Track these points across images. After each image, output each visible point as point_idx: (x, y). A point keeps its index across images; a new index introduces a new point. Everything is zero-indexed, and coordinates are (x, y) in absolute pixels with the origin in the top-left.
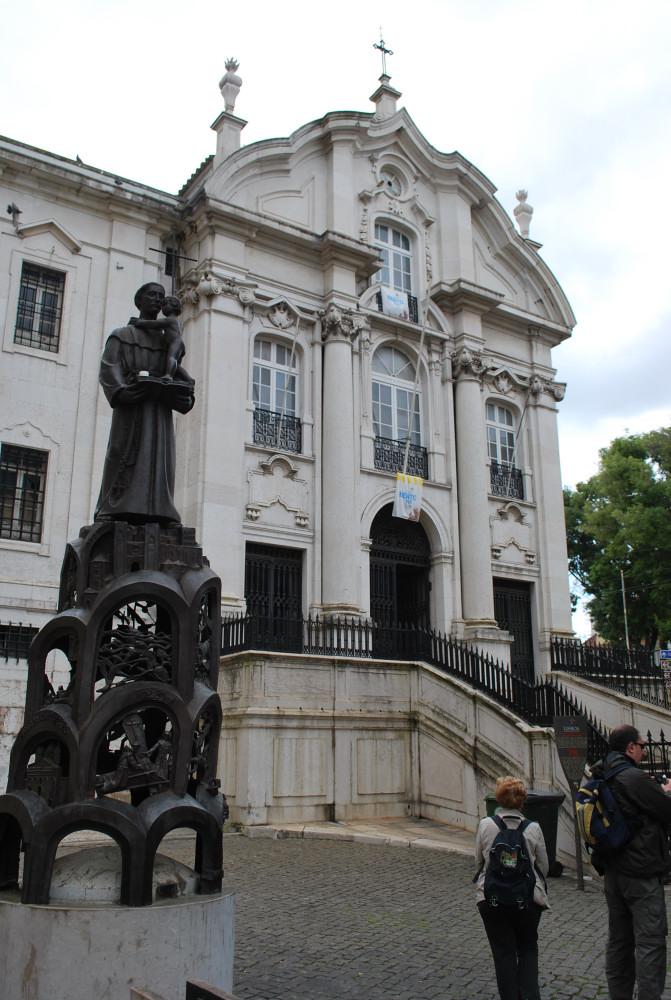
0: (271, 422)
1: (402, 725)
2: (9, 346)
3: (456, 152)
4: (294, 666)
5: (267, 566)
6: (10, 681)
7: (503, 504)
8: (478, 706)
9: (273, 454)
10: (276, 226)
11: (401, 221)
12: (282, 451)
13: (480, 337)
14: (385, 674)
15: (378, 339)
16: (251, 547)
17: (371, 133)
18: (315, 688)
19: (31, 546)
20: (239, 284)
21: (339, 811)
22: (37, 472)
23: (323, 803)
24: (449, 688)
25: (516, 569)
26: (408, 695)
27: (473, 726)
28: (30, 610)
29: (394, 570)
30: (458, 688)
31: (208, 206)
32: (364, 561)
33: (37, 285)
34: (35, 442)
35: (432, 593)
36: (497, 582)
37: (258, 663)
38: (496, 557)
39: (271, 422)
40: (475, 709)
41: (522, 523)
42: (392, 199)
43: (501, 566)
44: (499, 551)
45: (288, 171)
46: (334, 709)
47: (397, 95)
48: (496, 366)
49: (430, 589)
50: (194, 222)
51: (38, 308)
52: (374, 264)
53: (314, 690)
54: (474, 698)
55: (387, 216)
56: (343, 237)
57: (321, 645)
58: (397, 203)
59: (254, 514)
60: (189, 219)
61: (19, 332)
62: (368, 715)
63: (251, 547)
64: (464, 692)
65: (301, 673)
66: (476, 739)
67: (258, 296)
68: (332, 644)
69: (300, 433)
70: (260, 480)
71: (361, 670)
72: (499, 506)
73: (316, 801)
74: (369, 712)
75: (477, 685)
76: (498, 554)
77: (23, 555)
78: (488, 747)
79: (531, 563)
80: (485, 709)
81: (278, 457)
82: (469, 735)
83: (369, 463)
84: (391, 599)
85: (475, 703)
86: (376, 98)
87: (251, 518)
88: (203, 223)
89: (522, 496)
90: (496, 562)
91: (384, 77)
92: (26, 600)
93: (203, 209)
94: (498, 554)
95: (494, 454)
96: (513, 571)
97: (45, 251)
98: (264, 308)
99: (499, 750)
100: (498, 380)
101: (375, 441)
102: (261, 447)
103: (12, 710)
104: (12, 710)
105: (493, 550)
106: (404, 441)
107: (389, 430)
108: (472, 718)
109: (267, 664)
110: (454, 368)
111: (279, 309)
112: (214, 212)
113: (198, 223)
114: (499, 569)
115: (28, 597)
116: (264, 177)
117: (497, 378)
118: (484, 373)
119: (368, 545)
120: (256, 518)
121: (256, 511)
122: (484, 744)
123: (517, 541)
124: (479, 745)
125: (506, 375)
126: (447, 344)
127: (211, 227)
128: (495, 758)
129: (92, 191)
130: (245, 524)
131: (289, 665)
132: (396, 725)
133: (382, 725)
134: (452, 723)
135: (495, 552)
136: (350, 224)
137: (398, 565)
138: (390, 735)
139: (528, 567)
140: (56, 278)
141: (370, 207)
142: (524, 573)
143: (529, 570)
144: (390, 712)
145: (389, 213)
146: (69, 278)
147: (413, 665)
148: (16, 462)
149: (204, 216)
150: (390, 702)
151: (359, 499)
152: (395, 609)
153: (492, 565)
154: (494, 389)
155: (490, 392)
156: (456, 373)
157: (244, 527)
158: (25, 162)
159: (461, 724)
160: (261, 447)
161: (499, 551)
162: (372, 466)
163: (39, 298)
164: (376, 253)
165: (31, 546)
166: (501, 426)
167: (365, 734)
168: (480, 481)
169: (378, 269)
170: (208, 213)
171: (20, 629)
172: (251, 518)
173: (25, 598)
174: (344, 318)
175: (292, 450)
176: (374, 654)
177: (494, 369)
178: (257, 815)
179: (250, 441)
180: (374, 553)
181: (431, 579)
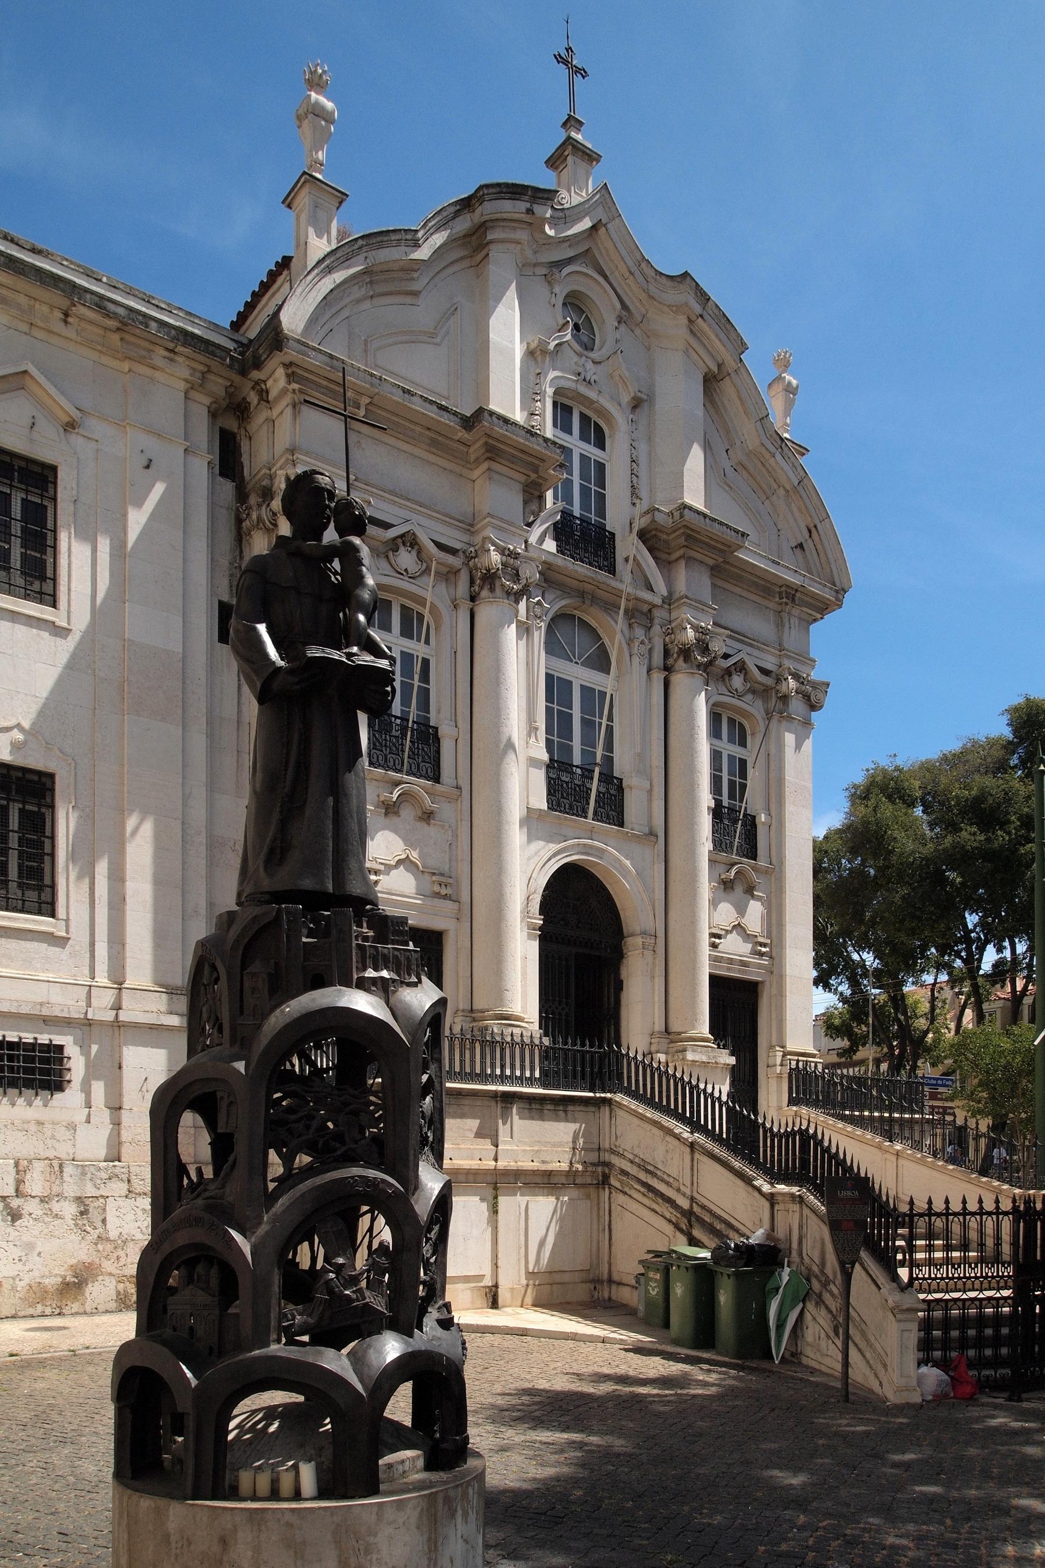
0: (394, 733)
3: (686, 274)
8: (697, 1156)
11: (592, 395)
14: (565, 1111)
22: (39, 806)
24: (655, 1131)
26: (596, 1140)
27: (688, 1184)
30: (669, 1132)
33: (11, 486)
35: (624, 996)
39: (394, 733)
40: (692, 1160)
46: (496, 1160)
47: (590, 157)
48: (730, 652)
49: (621, 989)
54: (692, 1146)
57: (478, 1071)
58: (590, 365)
64: (678, 1137)
66: (692, 1199)
69: (438, 752)
71: (533, 1106)
74: (543, 1162)
75: (695, 1126)
78: (710, 1212)
80: (705, 1159)
82: (684, 1195)
85: (692, 1152)
86: (555, 162)
88: (277, 381)
91: (571, 122)
99: (726, 1217)
101: (548, 766)
103: (36, 1164)
104: (36, 1164)
108: (688, 1171)
113: (269, 383)
118: (711, 663)
122: (703, 1207)
124: (696, 1209)
128: (719, 1226)
134: (663, 1180)
146: (66, 481)
147: (604, 1100)
149: (280, 372)
159: (671, 1180)
171: (33, 1046)
175: (427, 778)
176: (546, 1080)
181: (624, 974)
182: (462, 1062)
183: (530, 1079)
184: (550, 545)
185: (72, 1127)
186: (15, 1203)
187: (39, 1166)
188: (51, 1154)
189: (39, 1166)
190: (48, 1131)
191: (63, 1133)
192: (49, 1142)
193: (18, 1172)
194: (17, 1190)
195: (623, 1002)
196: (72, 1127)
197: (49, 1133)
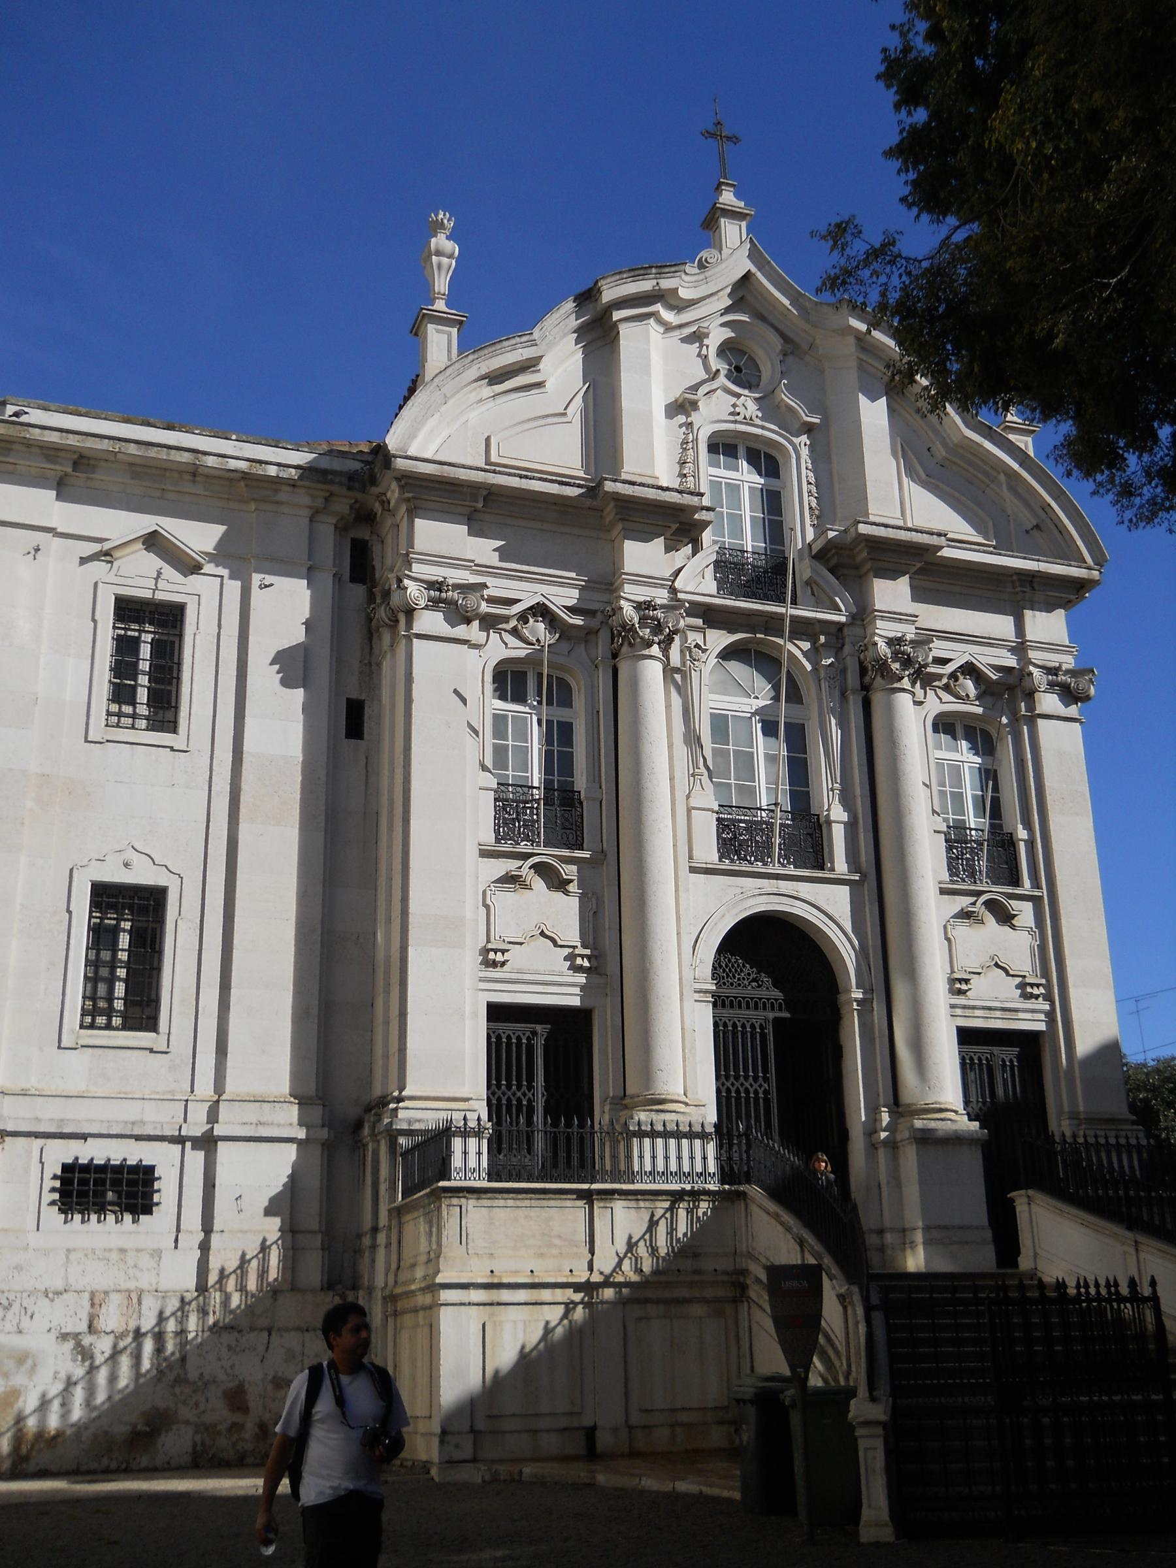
1: (721, 1292)
2: (98, 729)
4: (519, 1203)
5: (528, 1039)
6: (110, 1250)
7: (972, 899)
9: (526, 856)
10: (515, 482)
12: (542, 850)
13: (909, 611)
15: (719, 639)
16: (496, 1012)
17: (684, 293)
18: (559, 1237)
19: (115, 1037)
20: (456, 587)
21: (604, 1440)
23: (575, 1424)
25: (1004, 1009)
28: (138, 1138)
29: (769, 1031)
31: (395, 469)
32: (703, 1018)
34: (142, 875)
36: (966, 1036)
37: (455, 1201)
38: (961, 992)
41: (1013, 927)
42: (738, 396)
43: (974, 1008)
44: (967, 981)
45: (540, 385)
50: (385, 494)
51: (145, 666)
52: (696, 516)
53: (556, 1241)
55: (731, 426)
56: (633, 483)
59: (499, 957)
60: (375, 490)
61: (114, 708)
62: (697, 1278)
63: (496, 1012)
65: (534, 1213)
67: (492, 600)
68: (603, 1165)
70: (506, 900)
72: (964, 902)
73: (563, 1422)
76: (964, 987)
77: (129, 1052)
79: (1037, 997)
81: (536, 859)
83: (708, 853)
84: (766, 1079)
87: (494, 964)
89: (1016, 881)
90: (961, 1000)
92: (133, 1123)
93: (389, 474)
94: (964, 987)
95: (959, 808)
96: (998, 1014)
97: (143, 576)
98: (506, 619)
100: (957, 680)
102: (506, 847)
105: (952, 981)
106: (772, 807)
107: (752, 792)
109: (472, 1202)
110: (863, 670)
111: (534, 615)
112: (409, 477)
114: (968, 1012)
115: (138, 1118)
116: (500, 400)
117: (953, 676)
119: (706, 992)
120: (503, 964)
121: (503, 952)
123: (1004, 960)
125: (969, 669)
126: (846, 631)
127: (408, 500)
129: (213, 472)
130: (482, 974)
131: (510, 1203)
132: (709, 1293)
133: (685, 1293)
135: (958, 986)
136: (653, 456)
137: (776, 1020)
138: (698, 1310)
139: (1029, 1004)
140: (168, 618)
141: (695, 417)
142: (1021, 1015)
143: (1033, 1011)
144: (698, 1272)
145: (735, 422)
148: (113, 907)
150: (696, 1255)
151: (690, 912)
152: (774, 1096)
153: (953, 1006)
154: (946, 697)
155: (937, 703)
156: (867, 679)
157: (482, 980)
158: (105, 445)
160: (506, 847)
161: (967, 981)
162: (715, 857)
163: (145, 651)
164: (694, 501)
165: (115, 1037)
166: (966, 757)
167: (652, 1310)
168: (928, 860)
169: (705, 524)
170: (398, 479)
172: (494, 964)
173: (133, 1119)
174: (642, 619)
177: (944, 662)
178: (457, 1446)
179: (490, 838)
180: (719, 1002)
182: (614, 1157)
183: (652, 1173)
184: (710, 586)
185: (157, 1254)
186: (87, 1340)
187: (115, 1299)
188: (132, 1285)
189: (115, 1299)
190: (131, 1259)
191: (146, 1261)
192: (131, 1272)
193: (93, 1305)
194: (90, 1327)
195: (844, 1072)
196: (157, 1254)
197: (131, 1262)
